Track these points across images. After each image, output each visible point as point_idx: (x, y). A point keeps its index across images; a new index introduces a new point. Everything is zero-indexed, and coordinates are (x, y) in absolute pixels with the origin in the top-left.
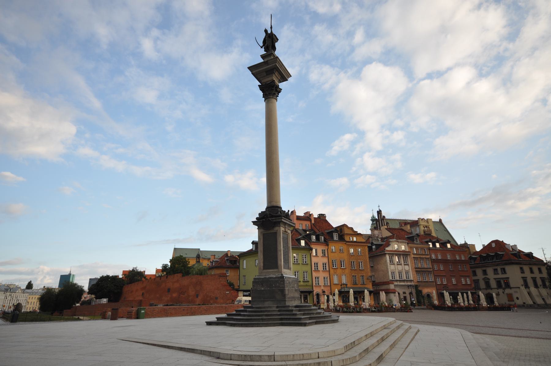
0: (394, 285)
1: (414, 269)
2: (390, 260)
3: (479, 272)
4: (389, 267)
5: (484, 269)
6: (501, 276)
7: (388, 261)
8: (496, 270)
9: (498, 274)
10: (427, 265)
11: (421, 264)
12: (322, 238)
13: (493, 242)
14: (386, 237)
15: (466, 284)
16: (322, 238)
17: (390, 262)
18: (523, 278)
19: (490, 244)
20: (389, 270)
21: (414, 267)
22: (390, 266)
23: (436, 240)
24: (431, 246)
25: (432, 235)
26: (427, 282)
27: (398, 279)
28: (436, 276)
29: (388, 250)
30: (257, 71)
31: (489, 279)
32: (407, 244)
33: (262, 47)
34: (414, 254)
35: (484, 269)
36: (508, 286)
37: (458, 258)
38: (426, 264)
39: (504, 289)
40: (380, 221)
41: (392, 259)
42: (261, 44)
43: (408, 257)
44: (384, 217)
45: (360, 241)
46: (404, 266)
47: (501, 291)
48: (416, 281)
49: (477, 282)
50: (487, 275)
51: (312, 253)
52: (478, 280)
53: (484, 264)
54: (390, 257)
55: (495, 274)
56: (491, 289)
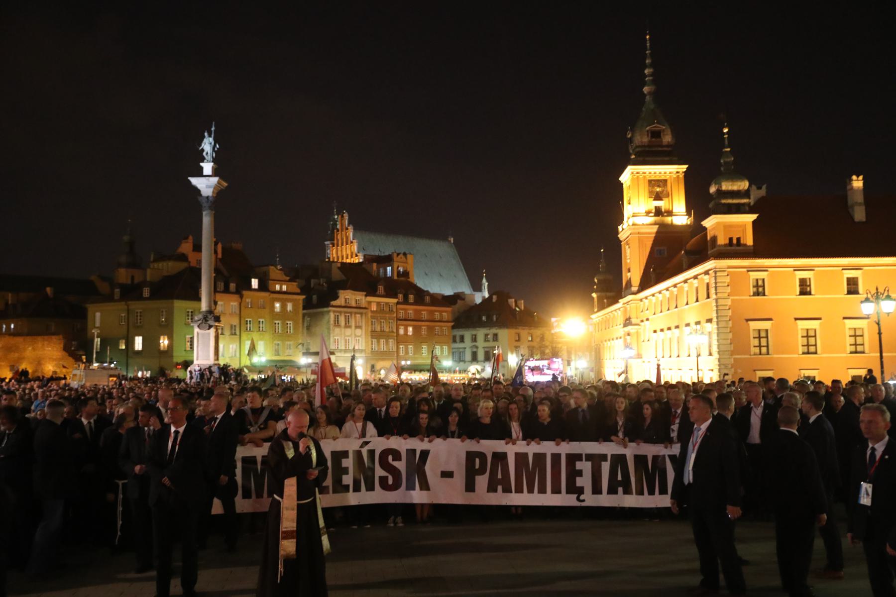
0: (336, 356)
1: (369, 334)
2: (335, 321)
7: (332, 322)
8: (486, 335)
9: (488, 341)
11: (381, 328)
12: (232, 286)
16: (232, 286)
17: (335, 324)
21: (370, 329)
22: (333, 330)
24: (401, 300)
27: (343, 348)
29: (334, 304)
31: (477, 347)
32: (364, 297)
34: (372, 312)
38: (388, 327)
41: (338, 318)
43: (364, 317)
45: (291, 291)
46: (355, 330)
48: (370, 352)
54: (335, 315)
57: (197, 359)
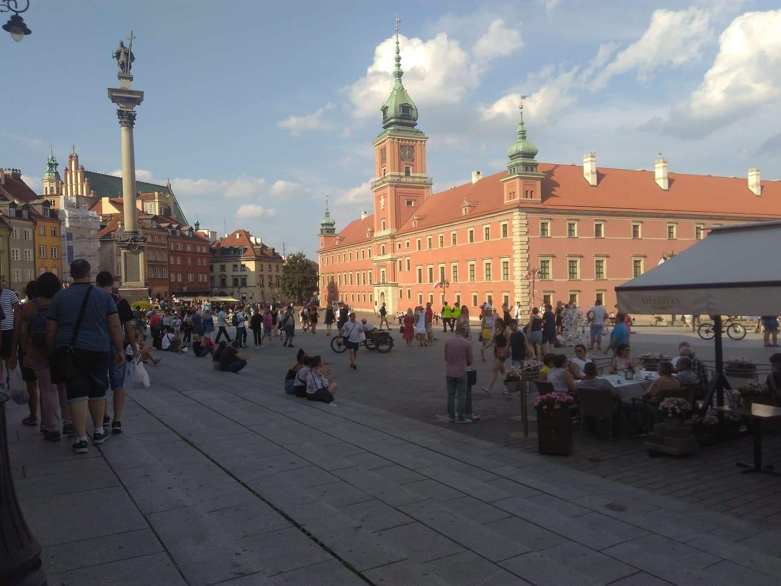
1: (146, 263)
3: (217, 267)
4: (115, 260)
5: (223, 264)
6: (239, 273)
9: (237, 271)
10: (163, 257)
13: (237, 232)
14: (111, 214)
15: (203, 282)
16: (25, 213)
18: (261, 275)
19: (234, 235)
20: (115, 263)
23: (177, 225)
25: (170, 216)
26: (159, 279)
28: (170, 272)
30: (118, 95)
31: (226, 276)
33: (114, 57)
35: (223, 264)
36: (244, 284)
37: (199, 250)
39: (240, 288)
40: (73, 173)
42: (114, 55)
44: (83, 168)
47: (236, 289)
49: (212, 279)
50: (225, 271)
51: (10, 235)
52: (214, 277)
53: (224, 258)
55: (234, 271)
56: (227, 287)
57: (126, 281)
